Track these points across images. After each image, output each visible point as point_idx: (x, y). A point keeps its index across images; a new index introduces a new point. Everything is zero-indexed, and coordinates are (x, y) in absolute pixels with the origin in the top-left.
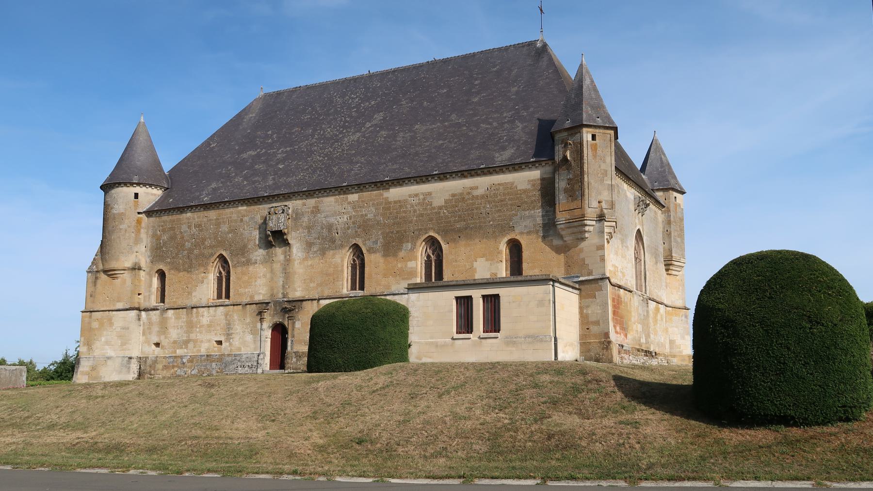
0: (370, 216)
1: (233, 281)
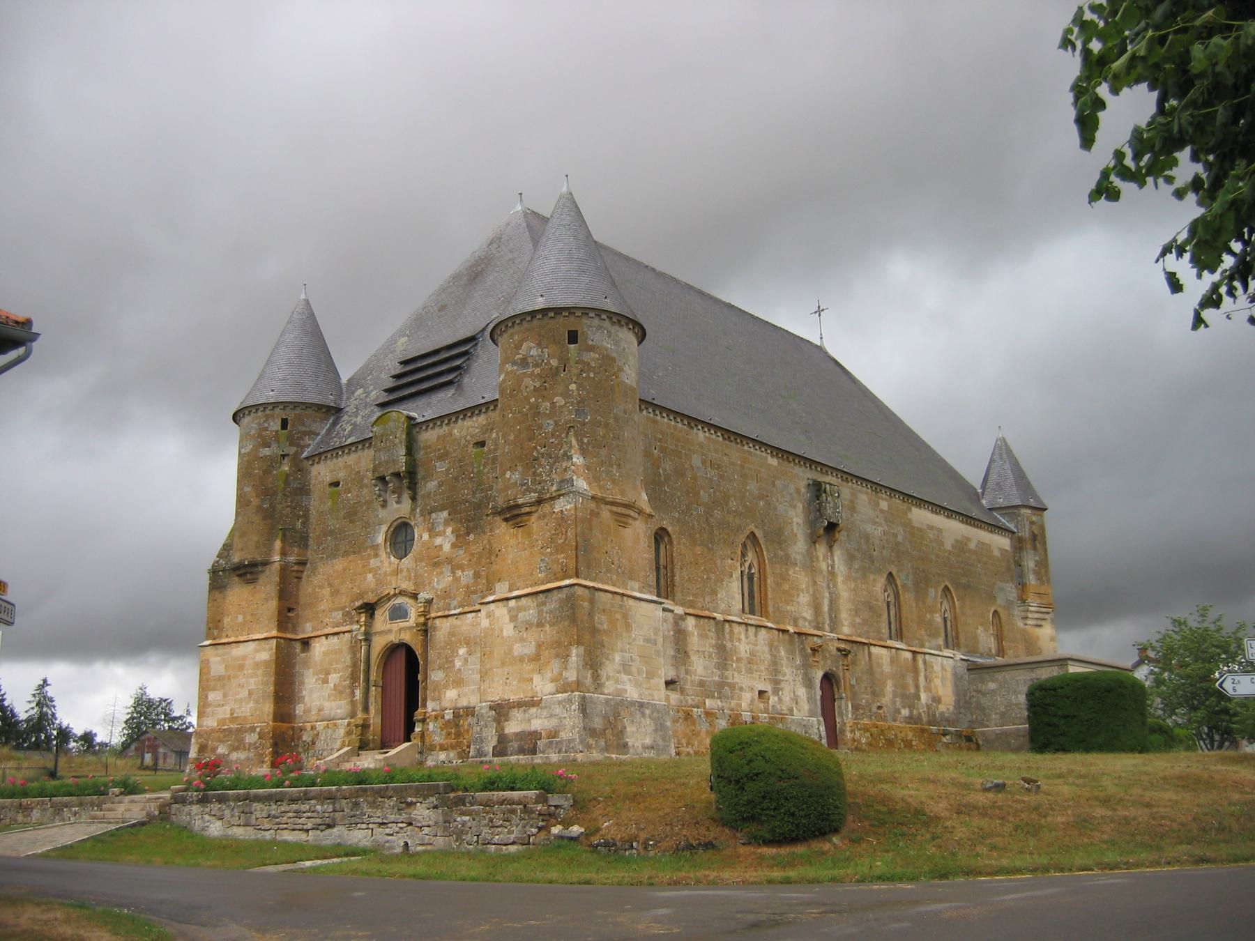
0: (900, 538)
1: (771, 587)
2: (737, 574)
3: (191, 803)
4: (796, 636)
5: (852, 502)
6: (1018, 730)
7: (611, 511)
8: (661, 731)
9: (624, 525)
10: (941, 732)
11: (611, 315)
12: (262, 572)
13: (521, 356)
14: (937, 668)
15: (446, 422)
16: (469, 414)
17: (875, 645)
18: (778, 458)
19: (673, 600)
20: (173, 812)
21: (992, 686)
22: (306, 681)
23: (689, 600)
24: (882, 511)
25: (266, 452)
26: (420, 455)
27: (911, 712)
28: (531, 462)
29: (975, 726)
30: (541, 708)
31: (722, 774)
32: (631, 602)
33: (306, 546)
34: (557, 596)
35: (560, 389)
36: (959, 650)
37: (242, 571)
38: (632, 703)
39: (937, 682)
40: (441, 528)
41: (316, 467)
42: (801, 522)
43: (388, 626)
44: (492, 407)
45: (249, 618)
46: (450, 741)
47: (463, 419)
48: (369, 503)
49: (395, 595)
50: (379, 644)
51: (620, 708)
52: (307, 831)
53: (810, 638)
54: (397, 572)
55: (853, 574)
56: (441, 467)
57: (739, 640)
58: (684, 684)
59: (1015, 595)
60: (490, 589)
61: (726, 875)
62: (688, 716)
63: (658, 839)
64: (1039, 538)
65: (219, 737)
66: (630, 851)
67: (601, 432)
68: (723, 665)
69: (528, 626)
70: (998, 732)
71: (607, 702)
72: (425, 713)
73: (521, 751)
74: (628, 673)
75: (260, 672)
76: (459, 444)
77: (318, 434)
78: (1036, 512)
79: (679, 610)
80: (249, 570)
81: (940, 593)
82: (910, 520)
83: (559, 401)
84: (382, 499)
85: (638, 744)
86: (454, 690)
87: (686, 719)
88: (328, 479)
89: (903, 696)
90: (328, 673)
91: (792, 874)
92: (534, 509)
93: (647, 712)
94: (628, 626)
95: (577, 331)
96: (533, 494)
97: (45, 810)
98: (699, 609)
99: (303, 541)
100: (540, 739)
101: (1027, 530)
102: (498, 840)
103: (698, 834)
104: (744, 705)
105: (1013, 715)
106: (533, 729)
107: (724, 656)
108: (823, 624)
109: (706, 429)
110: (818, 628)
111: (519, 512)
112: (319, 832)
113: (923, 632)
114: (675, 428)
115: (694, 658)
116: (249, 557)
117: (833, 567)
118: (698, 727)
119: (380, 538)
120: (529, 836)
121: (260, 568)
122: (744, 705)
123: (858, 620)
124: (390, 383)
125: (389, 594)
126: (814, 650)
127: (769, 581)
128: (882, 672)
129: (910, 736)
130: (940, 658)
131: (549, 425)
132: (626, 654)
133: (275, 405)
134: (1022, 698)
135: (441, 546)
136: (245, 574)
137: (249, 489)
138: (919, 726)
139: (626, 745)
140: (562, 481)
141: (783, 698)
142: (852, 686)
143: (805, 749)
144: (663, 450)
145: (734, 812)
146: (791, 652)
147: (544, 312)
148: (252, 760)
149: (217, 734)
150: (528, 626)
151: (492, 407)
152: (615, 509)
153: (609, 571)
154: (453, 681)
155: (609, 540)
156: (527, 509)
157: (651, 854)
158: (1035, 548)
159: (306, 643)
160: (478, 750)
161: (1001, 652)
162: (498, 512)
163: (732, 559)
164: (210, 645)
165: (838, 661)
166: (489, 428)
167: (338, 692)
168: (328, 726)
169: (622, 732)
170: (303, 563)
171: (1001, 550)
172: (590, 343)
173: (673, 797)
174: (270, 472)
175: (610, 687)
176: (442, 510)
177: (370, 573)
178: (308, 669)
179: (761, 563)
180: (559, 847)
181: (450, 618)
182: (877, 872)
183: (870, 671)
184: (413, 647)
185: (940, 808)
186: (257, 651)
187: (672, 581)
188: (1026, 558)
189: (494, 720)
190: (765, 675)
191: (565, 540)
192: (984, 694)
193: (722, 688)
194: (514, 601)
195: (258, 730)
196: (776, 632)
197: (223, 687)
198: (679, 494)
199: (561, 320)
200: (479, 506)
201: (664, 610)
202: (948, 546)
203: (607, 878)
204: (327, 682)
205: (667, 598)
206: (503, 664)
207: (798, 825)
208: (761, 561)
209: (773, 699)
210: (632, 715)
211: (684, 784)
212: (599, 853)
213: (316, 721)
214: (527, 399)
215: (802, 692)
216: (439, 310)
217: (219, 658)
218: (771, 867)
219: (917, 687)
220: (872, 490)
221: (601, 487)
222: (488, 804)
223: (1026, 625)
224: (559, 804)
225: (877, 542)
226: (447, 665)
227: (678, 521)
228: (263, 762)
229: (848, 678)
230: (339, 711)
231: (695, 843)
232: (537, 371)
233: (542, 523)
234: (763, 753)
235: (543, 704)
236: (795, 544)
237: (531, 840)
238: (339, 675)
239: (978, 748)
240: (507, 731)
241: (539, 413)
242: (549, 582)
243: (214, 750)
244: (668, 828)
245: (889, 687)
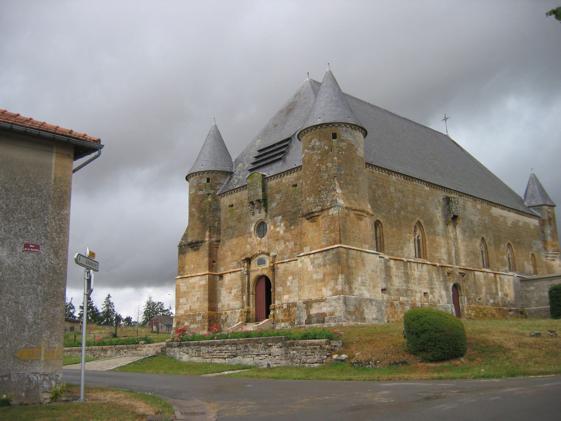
0: (487, 222)
1: (428, 245)
2: (412, 240)
3: (175, 347)
4: (440, 267)
5: (464, 206)
6: (545, 308)
7: (354, 214)
8: (380, 311)
9: (361, 220)
10: (509, 310)
11: (351, 125)
12: (201, 245)
13: (311, 145)
14: (506, 281)
15: (279, 176)
16: (289, 173)
17: (476, 271)
18: (429, 187)
19: (384, 253)
20: (167, 351)
21: (532, 288)
22: (222, 293)
23: (391, 253)
24: (478, 209)
25: (201, 193)
26: (268, 192)
27: (494, 301)
28: (318, 193)
29: (524, 307)
30: (326, 302)
31: (410, 330)
32: (365, 254)
33: (220, 234)
34: (331, 252)
35: (330, 159)
36: (516, 272)
37: (192, 246)
38: (367, 299)
39: (506, 287)
40: (279, 223)
41: (223, 198)
42: (441, 215)
43: (257, 268)
44: (299, 169)
45: (196, 266)
46: (285, 318)
47: (287, 175)
48: (247, 214)
49: (259, 254)
50: (253, 276)
51: (362, 302)
52: (225, 358)
53: (447, 268)
54: (260, 244)
55: (466, 239)
56: (278, 197)
57: (414, 270)
58: (390, 290)
59: (541, 246)
60: (302, 250)
61: (412, 376)
62: (392, 305)
63: (381, 360)
64: (552, 219)
65: (185, 318)
66: (368, 366)
67: (349, 178)
68: (407, 281)
69: (319, 266)
70: (535, 309)
71: (356, 299)
72: (275, 306)
73: (318, 322)
74: (365, 286)
75: (202, 289)
76: (285, 186)
77: (223, 184)
78: (550, 207)
79: (387, 257)
80: (195, 245)
81: (506, 246)
82: (491, 213)
83: (330, 165)
84: (252, 212)
85: (370, 318)
86: (287, 295)
87: (391, 306)
88: (228, 204)
89: (491, 294)
90: (231, 289)
91: (442, 375)
92: (320, 214)
93: (374, 303)
94: (364, 265)
95: (336, 133)
96: (319, 207)
97: (113, 351)
98: (395, 256)
99: (218, 231)
100: (326, 316)
101: (546, 216)
102: (309, 361)
103: (399, 357)
104: (417, 299)
105: (543, 302)
106: (323, 312)
107: (407, 277)
108: (453, 261)
109: (396, 175)
110: (450, 264)
112: (230, 359)
113: (498, 264)
114: (382, 175)
115: (394, 278)
116: (195, 239)
117: (456, 236)
118: (397, 310)
119: (252, 229)
120: (323, 359)
121: (200, 244)
122: (417, 299)
123: (468, 260)
124: (254, 160)
125: (257, 253)
126: (449, 274)
127: (427, 243)
128: (480, 283)
129: (494, 312)
130: (507, 276)
131: (326, 176)
132: (364, 278)
133: (204, 172)
134: (547, 294)
135: (279, 232)
137: (194, 209)
138: (498, 307)
139: (364, 318)
140: (332, 201)
141: (435, 295)
142: (467, 290)
143: (447, 318)
144: (377, 185)
145: (415, 347)
146: (438, 275)
147: (321, 125)
148: (200, 328)
149: (184, 317)
150: (319, 266)
151: (299, 169)
152: (356, 212)
153: (354, 240)
154: (287, 291)
155: (354, 227)
156: (317, 214)
157: (378, 367)
158: (550, 224)
159: (221, 276)
160: (299, 322)
161: (536, 273)
162: (304, 216)
163: (410, 233)
164: (180, 278)
165: (460, 278)
166: (299, 178)
168: (232, 313)
169: (362, 313)
170: (219, 241)
171: (534, 225)
172: (342, 138)
173: (387, 341)
174: (203, 202)
175: (356, 292)
176: (279, 216)
177: (248, 244)
178: (223, 287)
179: (423, 235)
180: (337, 364)
181: (284, 264)
182: (482, 374)
183: (475, 283)
184: (268, 277)
185: (510, 344)
186: (200, 280)
187: (383, 244)
188: (546, 229)
189: (306, 308)
190: (426, 285)
191: (335, 227)
192: (528, 292)
193: (407, 292)
194: (312, 255)
195: (202, 315)
196: (431, 266)
197: (186, 296)
198: (385, 205)
199: (329, 129)
200: (295, 213)
201: (380, 257)
202: (509, 224)
203: (359, 378)
205: (381, 252)
206: (309, 283)
207: (444, 353)
208: (423, 233)
209: (431, 296)
210: (367, 305)
211: (392, 335)
212: (354, 367)
213: (227, 310)
214: (315, 165)
215: (444, 293)
216: (274, 127)
217: (183, 284)
218: (433, 372)
219: (497, 289)
220: (473, 200)
221: (349, 203)
222: (304, 345)
223: (547, 260)
224: (336, 345)
225: (476, 223)
226: (284, 284)
227: (385, 217)
229: (464, 286)
230: (237, 306)
231: (398, 362)
232: (319, 152)
233: (324, 220)
234: (428, 321)
235: (327, 301)
236: (438, 226)
237: (324, 361)
238: (236, 290)
239: (526, 317)
240: (311, 313)
241: (320, 171)
242: (328, 246)
244: (385, 355)
245: (484, 290)
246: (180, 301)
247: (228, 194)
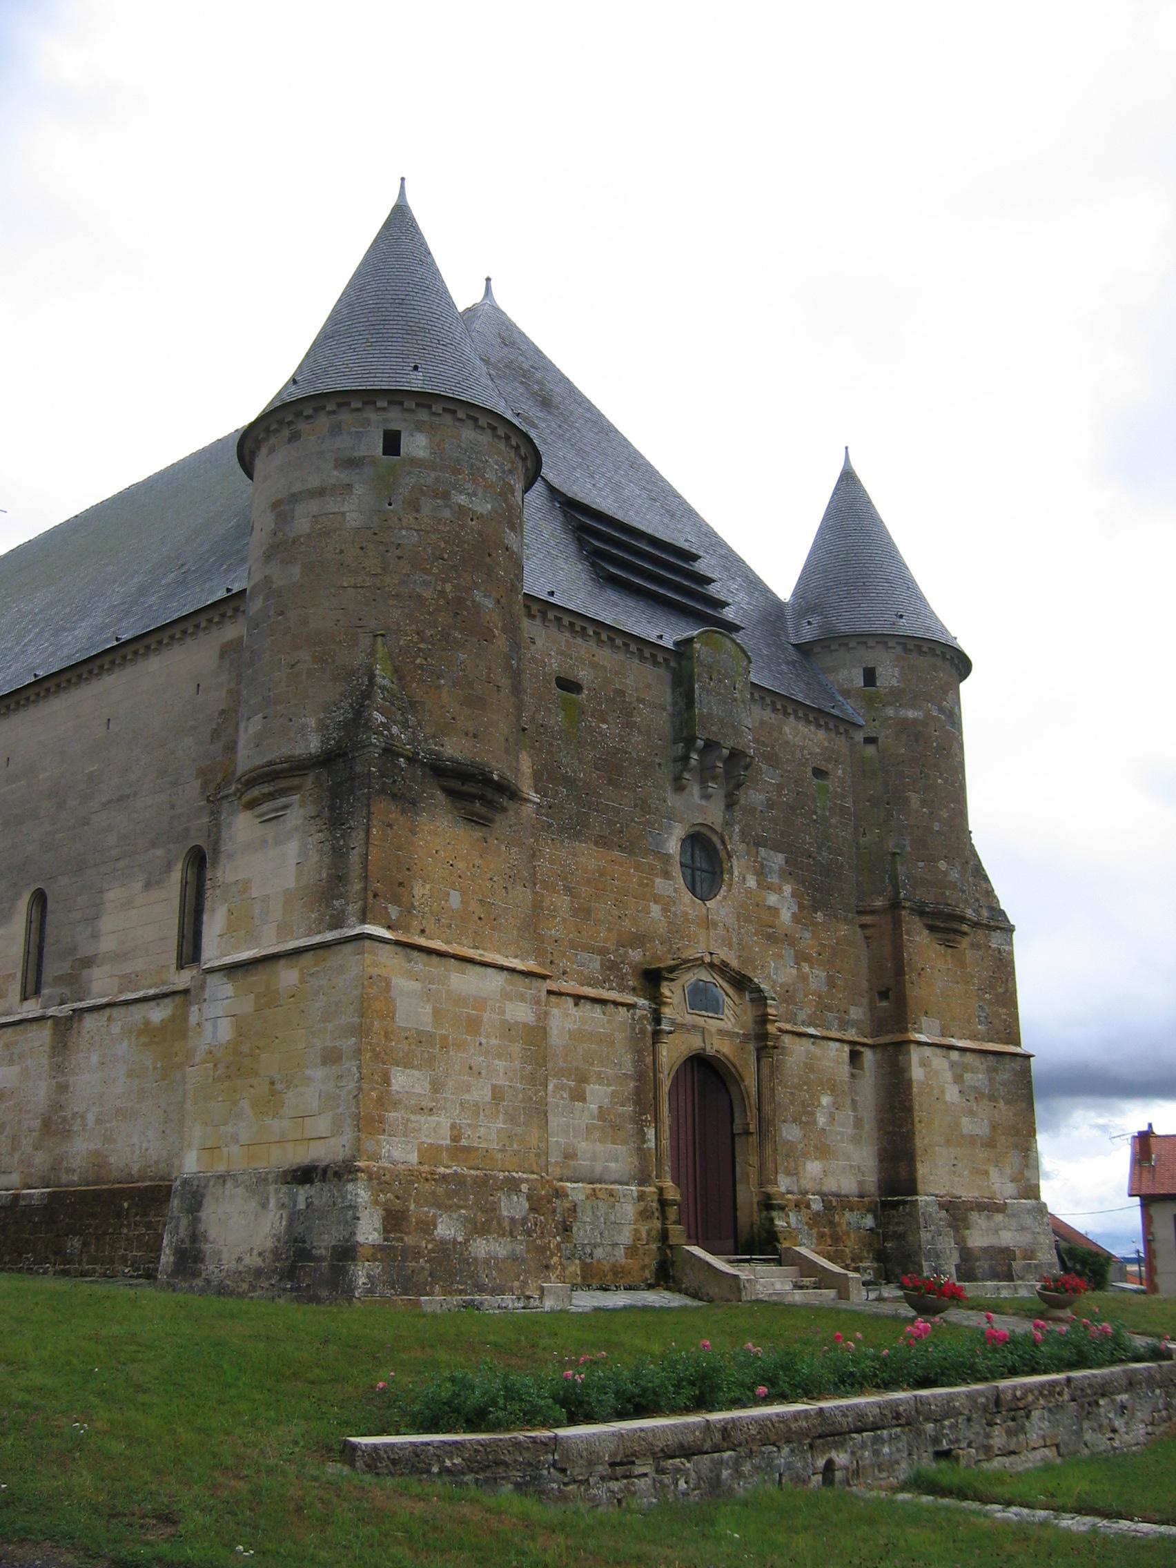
30: (1008, 1216)
45: (474, 906)
56: (770, 777)
65: (434, 1193)
73: (995, 1276)
75: (516, 1048)
86: (817, 1162)
90: (583, 1079)
97: (1060, 1407)
106: (1004, 1244)
111: (955, 926)
136: (470, 797)
148: (524, 1261)
150: (979, 1096)
167: (608, 1125)
176: (776, 849)
177: (656, 902)
181: (804, 1040)
186: (507, 996)
195: (524, 1187)
197: (430, 1062)
204: (582, 1098)
206: (948, 1142)
217: (415, 986)
226: (805, 1117)
228: (547, 1267)
230: (612, 1165)
235: (1009, 1211)
240: (970, 1244)
243: (427, 1227)
246: (395, 1086)
247: (566, 622)
